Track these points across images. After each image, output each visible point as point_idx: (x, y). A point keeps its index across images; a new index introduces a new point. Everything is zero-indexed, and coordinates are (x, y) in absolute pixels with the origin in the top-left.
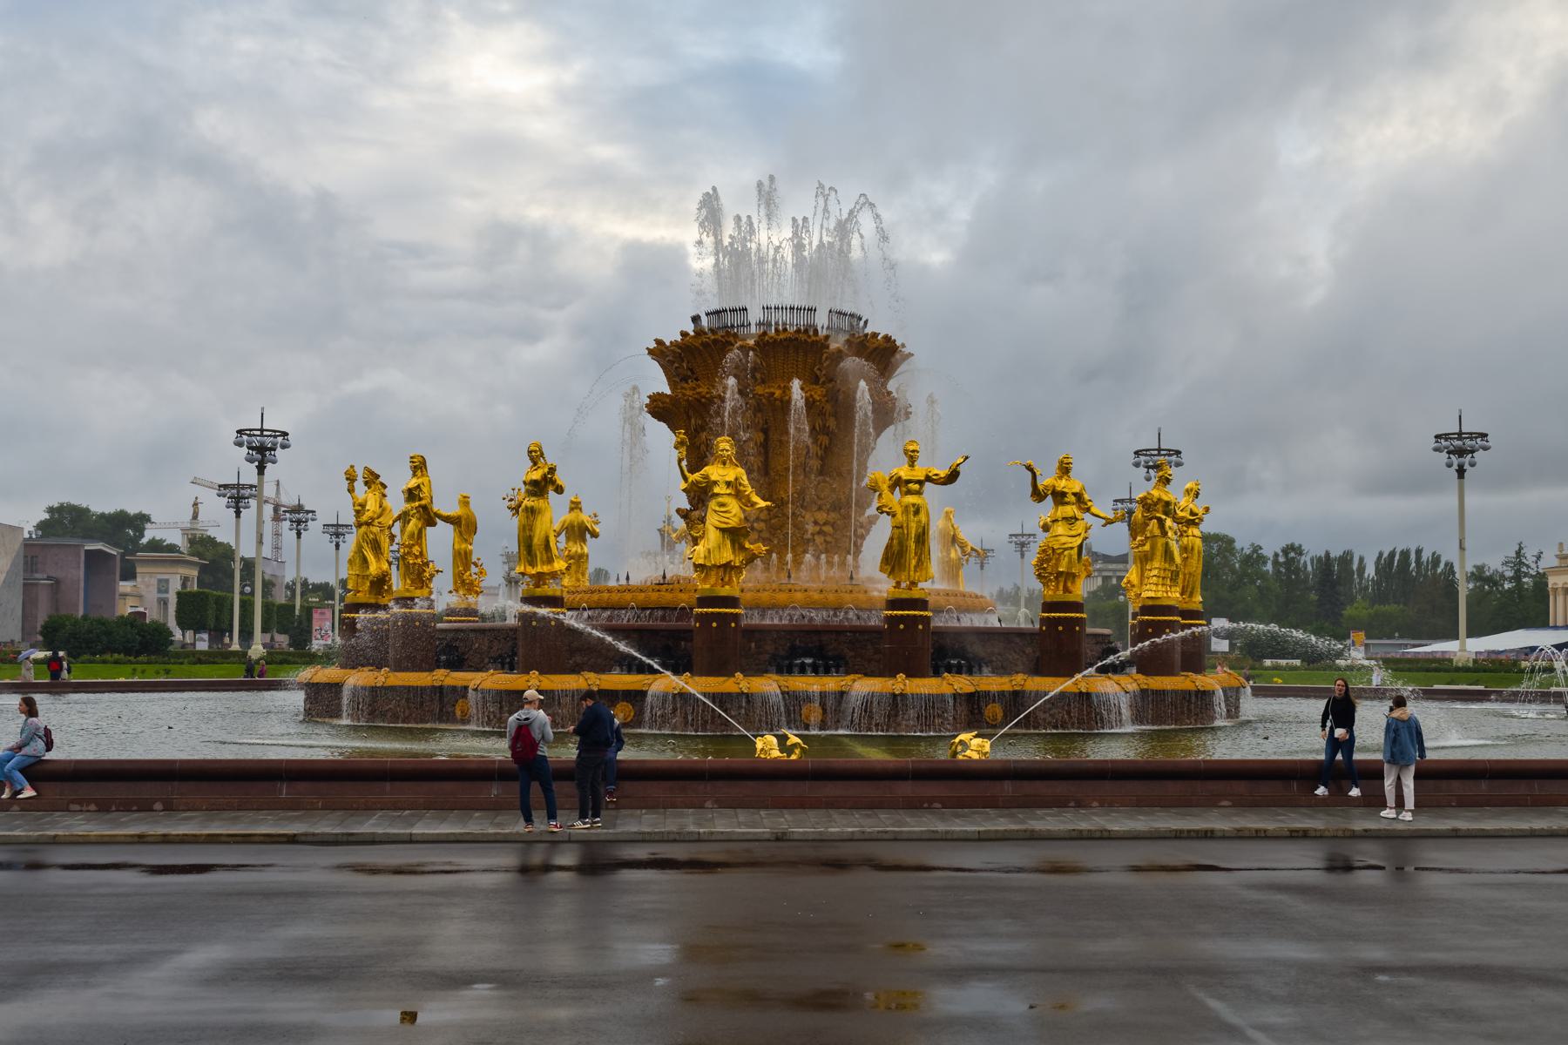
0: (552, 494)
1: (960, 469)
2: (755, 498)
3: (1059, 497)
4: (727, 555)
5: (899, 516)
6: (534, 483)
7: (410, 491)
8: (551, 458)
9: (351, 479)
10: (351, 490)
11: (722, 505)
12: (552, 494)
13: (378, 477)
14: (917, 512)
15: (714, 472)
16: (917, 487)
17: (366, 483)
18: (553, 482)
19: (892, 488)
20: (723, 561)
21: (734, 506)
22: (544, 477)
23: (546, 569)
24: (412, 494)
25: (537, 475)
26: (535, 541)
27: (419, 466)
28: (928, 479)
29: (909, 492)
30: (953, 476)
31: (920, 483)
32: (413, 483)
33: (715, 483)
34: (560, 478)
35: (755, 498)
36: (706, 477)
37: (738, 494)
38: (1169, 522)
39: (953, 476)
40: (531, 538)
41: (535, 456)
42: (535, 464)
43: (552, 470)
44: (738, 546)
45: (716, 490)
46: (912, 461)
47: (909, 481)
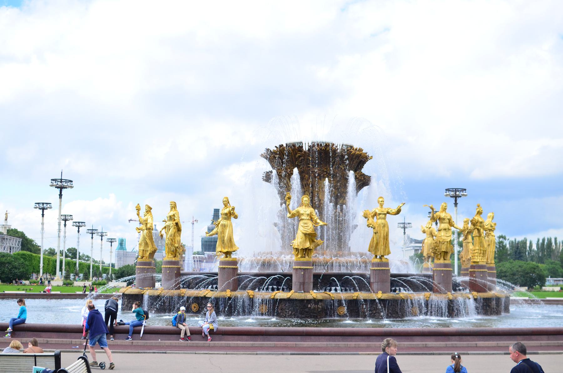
0: (232, 218)
1: (402, 208)
2: (318, 221)
4: (308, 245)
5: (376, 228)
6: (226, 214)
7: (170, 217)
8: (232, 204)
11: (306, 224)
12: (232, 218)
13: (151, 209)
14: (384, 226)
16: (384, 216)
18: (233, 214)
19: (373, 217)
20: (306, 247)
21: (310, 224)
22: (230, 212)
23: (230, 250)
24: (171, 218)
26: (226, 238)
28: (388, 213)
29: (380, 218)
30: (398, 212)
31: (385, 214)
32: (172, 213)
33: (302, 214)
34: (236, 212)
35: (318, 221)
36: (298, 212)
37: (311, 219)
38: (482, 230)
39: (398, 212)
40: (224, 237)
42: (226, 206)
43: (233, 209)
44: (312, 241)
45: (303, 217)
46: (382, 205)
47: (380, 214)
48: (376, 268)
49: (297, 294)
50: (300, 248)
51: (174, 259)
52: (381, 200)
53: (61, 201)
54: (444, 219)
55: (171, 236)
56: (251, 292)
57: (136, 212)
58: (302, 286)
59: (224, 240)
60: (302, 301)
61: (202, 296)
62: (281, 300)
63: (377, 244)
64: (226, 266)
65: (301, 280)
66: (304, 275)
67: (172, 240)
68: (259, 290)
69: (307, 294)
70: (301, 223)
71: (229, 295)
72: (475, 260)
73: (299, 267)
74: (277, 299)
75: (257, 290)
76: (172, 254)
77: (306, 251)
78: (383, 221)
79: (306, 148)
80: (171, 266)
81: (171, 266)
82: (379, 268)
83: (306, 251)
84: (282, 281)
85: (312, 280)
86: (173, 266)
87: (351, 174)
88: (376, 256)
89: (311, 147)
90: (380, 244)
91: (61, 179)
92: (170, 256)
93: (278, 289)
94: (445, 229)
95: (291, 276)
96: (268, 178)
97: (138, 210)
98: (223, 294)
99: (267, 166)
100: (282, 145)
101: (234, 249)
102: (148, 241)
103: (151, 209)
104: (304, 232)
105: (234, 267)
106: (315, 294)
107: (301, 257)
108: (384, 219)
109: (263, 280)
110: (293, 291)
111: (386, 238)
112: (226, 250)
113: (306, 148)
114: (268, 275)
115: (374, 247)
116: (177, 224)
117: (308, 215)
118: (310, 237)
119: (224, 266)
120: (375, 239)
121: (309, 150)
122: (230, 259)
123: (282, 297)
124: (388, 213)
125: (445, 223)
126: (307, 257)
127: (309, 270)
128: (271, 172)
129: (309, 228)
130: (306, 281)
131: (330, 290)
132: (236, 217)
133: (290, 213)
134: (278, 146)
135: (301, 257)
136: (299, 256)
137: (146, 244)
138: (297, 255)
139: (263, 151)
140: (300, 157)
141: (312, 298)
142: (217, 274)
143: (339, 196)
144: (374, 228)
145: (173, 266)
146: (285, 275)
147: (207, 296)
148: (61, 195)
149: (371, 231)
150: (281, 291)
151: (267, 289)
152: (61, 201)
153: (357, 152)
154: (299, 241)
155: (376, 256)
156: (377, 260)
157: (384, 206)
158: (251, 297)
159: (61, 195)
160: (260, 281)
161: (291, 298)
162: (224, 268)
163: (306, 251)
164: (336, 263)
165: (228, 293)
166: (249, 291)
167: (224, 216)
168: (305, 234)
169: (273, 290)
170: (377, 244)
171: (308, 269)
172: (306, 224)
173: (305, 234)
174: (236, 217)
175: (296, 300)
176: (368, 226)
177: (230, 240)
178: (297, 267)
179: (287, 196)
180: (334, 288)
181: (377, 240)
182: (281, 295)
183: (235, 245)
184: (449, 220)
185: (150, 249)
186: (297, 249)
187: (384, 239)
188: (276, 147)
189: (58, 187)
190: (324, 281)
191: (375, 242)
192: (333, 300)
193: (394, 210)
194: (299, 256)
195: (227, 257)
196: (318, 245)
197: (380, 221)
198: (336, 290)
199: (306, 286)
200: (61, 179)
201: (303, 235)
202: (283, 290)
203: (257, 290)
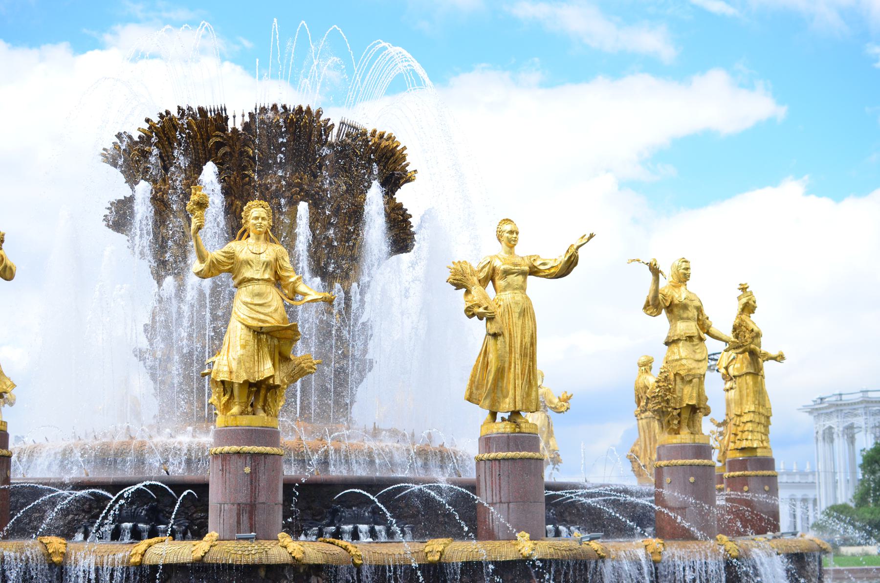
3: (673, 309)
4: (266, 369)
5: (498, 318)
11: (259, 295)
15: (243, 248)
19: (484, 282)
20: (258, 377)
31: (524, 274)
33: (248, 263)
36: (231, 256)
37: (278, 281)
39: (571, 263)
44: (282, 358)
45: (248, 273)
46: (511, 245)
47: (507, 273)
48: (501, 455)
49: (230, 545)
50: (241, 377)
52: (508, 227)
54: (685, 307)
56: (56, 543)
58: (245, 518)
60: (250, 570)
62: (169, 568)
63: (501, 373)
65: (243, 497)
66: (253, 477)
69: (267, 544)
70: (244, 294)
72: (745, 444)
73: (235, 448)
74: (154, 568)
75: (79, 537)
78: (518, 297)
79: (236, 123)
82: (510, 454)
83: (259, 392)
84: (173, 505)
85: (280, 497)
88: (494, 415)
90: (506, 374)
93: (153, 533)
94: (690, 338)
95: (202, 488)
96: (120, 217)
99: (116, 185)
100: (168, 113)
104: (255, 324)
106: (286, 548)
107: (242, 413)
108: (523, 288)
110: (212, 534)
111: (529, 354)
113: (236, 123)
114: (115, 487)
115: (488, 387)
117: (267, 265)
118: (275, 340)
120: (492, 357)
121: (247, 126)
123: (172, 559)
124: (534, 271)
125: (688, 319)
126: (262, 414)
127: (270, 460)
128: (130, 200)
129: (273, 311)
130: (262, 498)
133: (202, 258)
134: (156, 119)
135: (242, 413)
136: (235, 409)
138: (227, 406)
139: (109, 141)
140: (219, 145)
143: (337, 257)
144: (490, 319)
146: (179, 486)
149: (479, 328)
150: (168, 539)
153: (384, 144)
154: (234, 358)
155: (494, 415)
156: (501, 427)
157: (519, 250)
158: (56, 559)
160: (87, 510)
161: (208, 559)
164: (337, 451)
166: (46, 540)
168: (258, 332)
169: (136, 535)
170: (501, 373)
171: (266, 455)
172: (259, 295)
173: (258, 332)
175: (228, 568)
176: (470, 313)
178: (226, 449)
179: (193, 198)
180: (348, 528)
181: (500, 358)
182: (167, 550)
184: (699, 309)
186: (226, 386)
187: (524, 355)
188: (147, 120)
190: (317, 503)
191: (493, 367)
192: (359, 568)
193: (556, 257)
194: (235, 409)
196: (302, 372)
197: (507, 297)
198: (355, 535)
199: (260, 517)
201: (250, 336)
202: (173, 535)
203: (79, 537)
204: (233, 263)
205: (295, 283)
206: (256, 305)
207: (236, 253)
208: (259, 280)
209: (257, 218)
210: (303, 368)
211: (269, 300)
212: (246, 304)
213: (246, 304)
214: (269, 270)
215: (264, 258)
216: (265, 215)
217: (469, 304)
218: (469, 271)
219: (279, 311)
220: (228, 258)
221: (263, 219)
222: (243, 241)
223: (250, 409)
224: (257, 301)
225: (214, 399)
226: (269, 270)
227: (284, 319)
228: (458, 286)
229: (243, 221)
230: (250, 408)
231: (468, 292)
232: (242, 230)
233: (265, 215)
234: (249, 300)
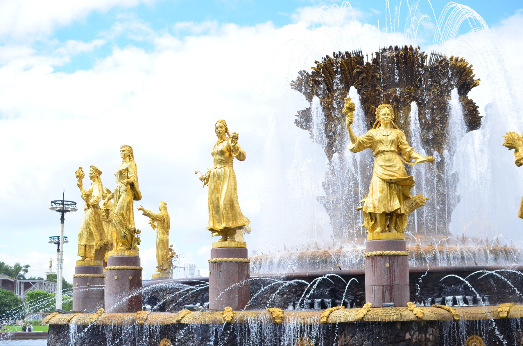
0: (236, 161)
4: (396, 204)
6: (222, 153)
9: (80, 177)
10: (80, 186)
11: (389, 160)
12: (236, 161)
13: (100, 173)
15: (377, 133)
17: (92, 178)
20: (391, 209)
21: (398, 162)
23: (231, 225)
25: (223, 146)
27: (128, 154)
32: (123, 167)
33: (381, 141)
34: (241, 144)
36: (371, 138)
37: (400, 152)
40: (218, 199)
41: (222, 131)
43: (235, 138)
44: (404, 197)
45: (381, 148)
49: (379, 310)
51: (127, 254)
53: (63, 227)
55: (122, 208)
56: (277, 311)
57: (76, 180)
58: (387, 294)
59: (218, 206)
60: (391, 325)
61: (174, 322)
62: (344, 326)
64: (224, 259)
66: (391, 269)
67: (122, 215)
68: (294, 306)
69: (401, 309)
70: (379, 161)
71: (229, 319)
73: (379, 252)
74: (334, 324)
75: (290, 307)
76: (123, 244)
77: (391, 220)
79: (368, 59)
80: (121, 267)
81: (121, 267)
83: (392, 218)
84: (344, 287)
86: (125, 267)
87: (454, 100)
89: (379, 57)
91: (63, 201)
92: (120, 247)
93: (334, 304)
95: (361, 277)
96: (305, 119)
97: (80, 177)
98: (218, 315)
99: (300, 102)
100: (328, 57)
101: (240, 224)
102: (93, 228)
103: (100, 173)
104: (387, 178)
105: (241, 260)
106: (414, 311)
107: (382, 231)
109: (302, 286)
110: (368, 304)
112: (220, 227)
113: (368, 59)
114: (310, 278)
116: (132, 185)
117: (392, 142)
118: (400, 186)
119: (219, 259)
121: (375, 61)
122: (233, 244)
123: (344, 319)
126: (394, 231)
127: (400, 258)
128: (308, 110)
129: (398, 171)
130: (397, 282)
131: (443, 303)
132: (241, 157)
133: (353, 141)
134: (321, 61)
135: (382, 231)
136: (378, 229)
137: (90, 234)
138: (373, 228)
139: (295, 76)
140: (359, 73)
141: (413, 318)
142: (207, 280)
143: (435, 136)
145: (125, 267)
146: (347, 277)
147: (183, 321)
148: (62, 220)
150: (341, 307)
151: (312, 306)
152: (63, 227)
153: (459, 64)
154: (376, 199)
158: (278, 321)
159: (62, 220)
160: (294, 291)
161: (366, 319)
162: (221, 262)
163: (391, 220)
165: (228, 314)
166: (272, 310)
167: (218, 157)
168: (389, 183)
169: (323, 306)
171: (398, 256)
172: (389, 160)
173: (389, 183)
174: (241, 157)
175: (378, 324)
177: (232, 205)
178: (374, 253)
179: (346, 105)
180: (450, 298)
182: (341, 314)
183: (241, 215)
185: (96, 243)
186: (372, 216)
188: (316, 62)
189: (59, 211)
190: (430, 284)
192: (457, 321)
194: (378, 229)
195: (226, 240)
198: (455, 302)
199: (396, 293)
200: (63, 201)
201: (385, 186)
202: (345, 305)
203: (290, 307)
204: (372, 142)
205: (410, 152)
206: (387, 166)
207: (374, 136)
208: (388, 151)
209: (384, 115)
210: (417, 203)
211: (395, 163)
212: (381, 166)
213: (381, 166)
214: (393, 145)
215: (390, 138)
216: (389, 113)
217: (518, 158)
218: (516, 138)
219: (401, 169)
220: (369, 139)
221: (388, 115)
222: (377, 129)
223: (387, 229)
224: (388, 164)
225: (365, 224)
226: (393, 145)
227: (404, 174)
228: (510, 147)
229: (376, 117)
230: (387, 229)
231: (517, 151)
232: (376, 122)
233: (389, 113)
234: (383, 164)
